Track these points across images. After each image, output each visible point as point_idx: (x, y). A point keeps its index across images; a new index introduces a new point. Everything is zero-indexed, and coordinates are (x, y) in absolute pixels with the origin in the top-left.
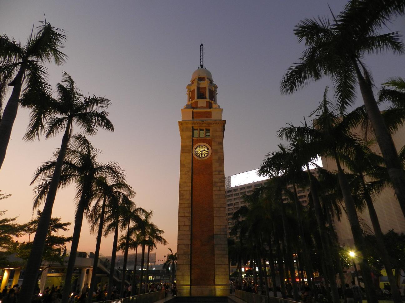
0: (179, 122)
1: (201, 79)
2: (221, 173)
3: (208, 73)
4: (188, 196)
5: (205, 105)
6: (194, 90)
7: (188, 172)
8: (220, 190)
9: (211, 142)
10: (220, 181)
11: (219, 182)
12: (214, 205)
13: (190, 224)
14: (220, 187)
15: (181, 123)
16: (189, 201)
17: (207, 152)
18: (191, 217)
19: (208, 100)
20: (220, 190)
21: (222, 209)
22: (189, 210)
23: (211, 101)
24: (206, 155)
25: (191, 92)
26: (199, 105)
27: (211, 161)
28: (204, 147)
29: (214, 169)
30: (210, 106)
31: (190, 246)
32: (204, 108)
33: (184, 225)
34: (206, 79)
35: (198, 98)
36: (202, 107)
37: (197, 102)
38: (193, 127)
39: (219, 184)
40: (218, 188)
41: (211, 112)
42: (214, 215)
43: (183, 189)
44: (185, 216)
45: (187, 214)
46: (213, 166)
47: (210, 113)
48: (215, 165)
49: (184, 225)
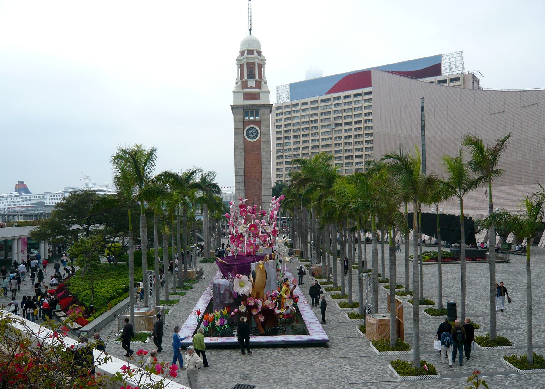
0: (231, 105)
1: (251, 52)
2: (268, 154)
3: (258, 43)
4: (242, 173)
5: (254, 86)
7: (241, 152)
15: (233, 107)
16: (243, 178)
19: (257, 78)
21: (268, 183)
22: (243, 184)
23: (260, 80)
25: (241, 67)
26: (249, 86)
29: (262, 150)
30: (258, 85)
32: (254, 88)
34: (255, 53)
35: (247, 78)
36: (251, 87)
39: (266, 163)
43: (238, 168)
45: (241, 188)
48: (263, 146)
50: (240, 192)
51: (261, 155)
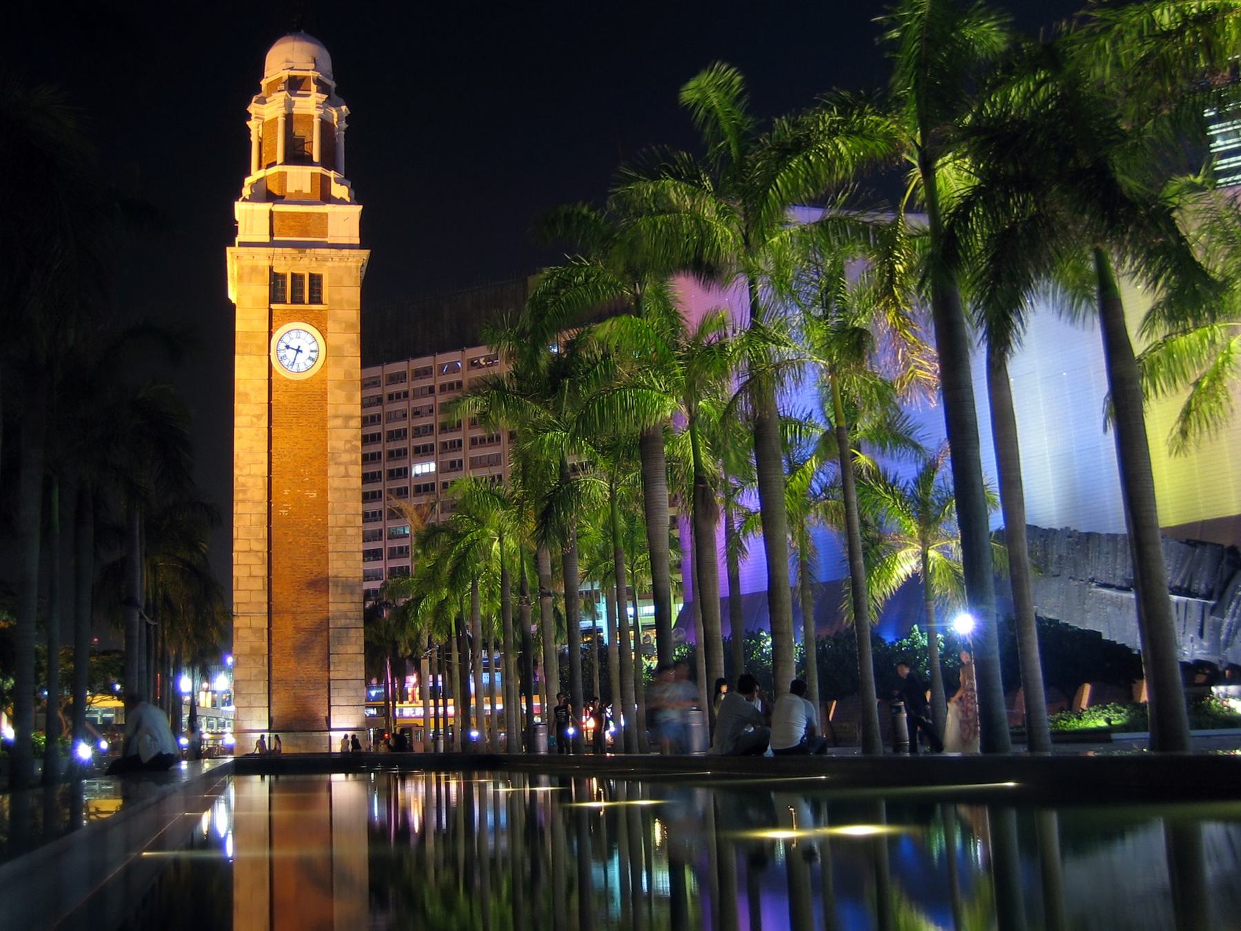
5: (307, 189)
6: (275, 120)
7: (259, 417)
8: (347, 475)
9: (326, 319)
10: (348, 446)
11: (346, 451)
12: (331, 520)
13: (265, 573)
14: (346, 465)
16: (263, 509)
17: (314, 355)
18: (269, 552)
20: (347, 475)
21: (350, 531)
24: (310, 363)
26: (290, 189)
27: (324, 382)
28: (303, 334)
29: (330, 411)
31: (266, 632)
33: (251, 576)
37: (283, 175)
38: (271, 269)
39: (345, 457)
40: (342, 469)
41: (326, 214)
42: (330, 548)
44: (250, 551)
46: (330, 399)
47: (323, 217)
49: (251, 576)
50: (253, 560)
51: (324, 428)
